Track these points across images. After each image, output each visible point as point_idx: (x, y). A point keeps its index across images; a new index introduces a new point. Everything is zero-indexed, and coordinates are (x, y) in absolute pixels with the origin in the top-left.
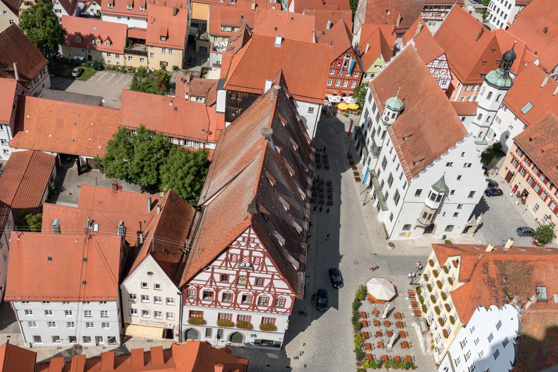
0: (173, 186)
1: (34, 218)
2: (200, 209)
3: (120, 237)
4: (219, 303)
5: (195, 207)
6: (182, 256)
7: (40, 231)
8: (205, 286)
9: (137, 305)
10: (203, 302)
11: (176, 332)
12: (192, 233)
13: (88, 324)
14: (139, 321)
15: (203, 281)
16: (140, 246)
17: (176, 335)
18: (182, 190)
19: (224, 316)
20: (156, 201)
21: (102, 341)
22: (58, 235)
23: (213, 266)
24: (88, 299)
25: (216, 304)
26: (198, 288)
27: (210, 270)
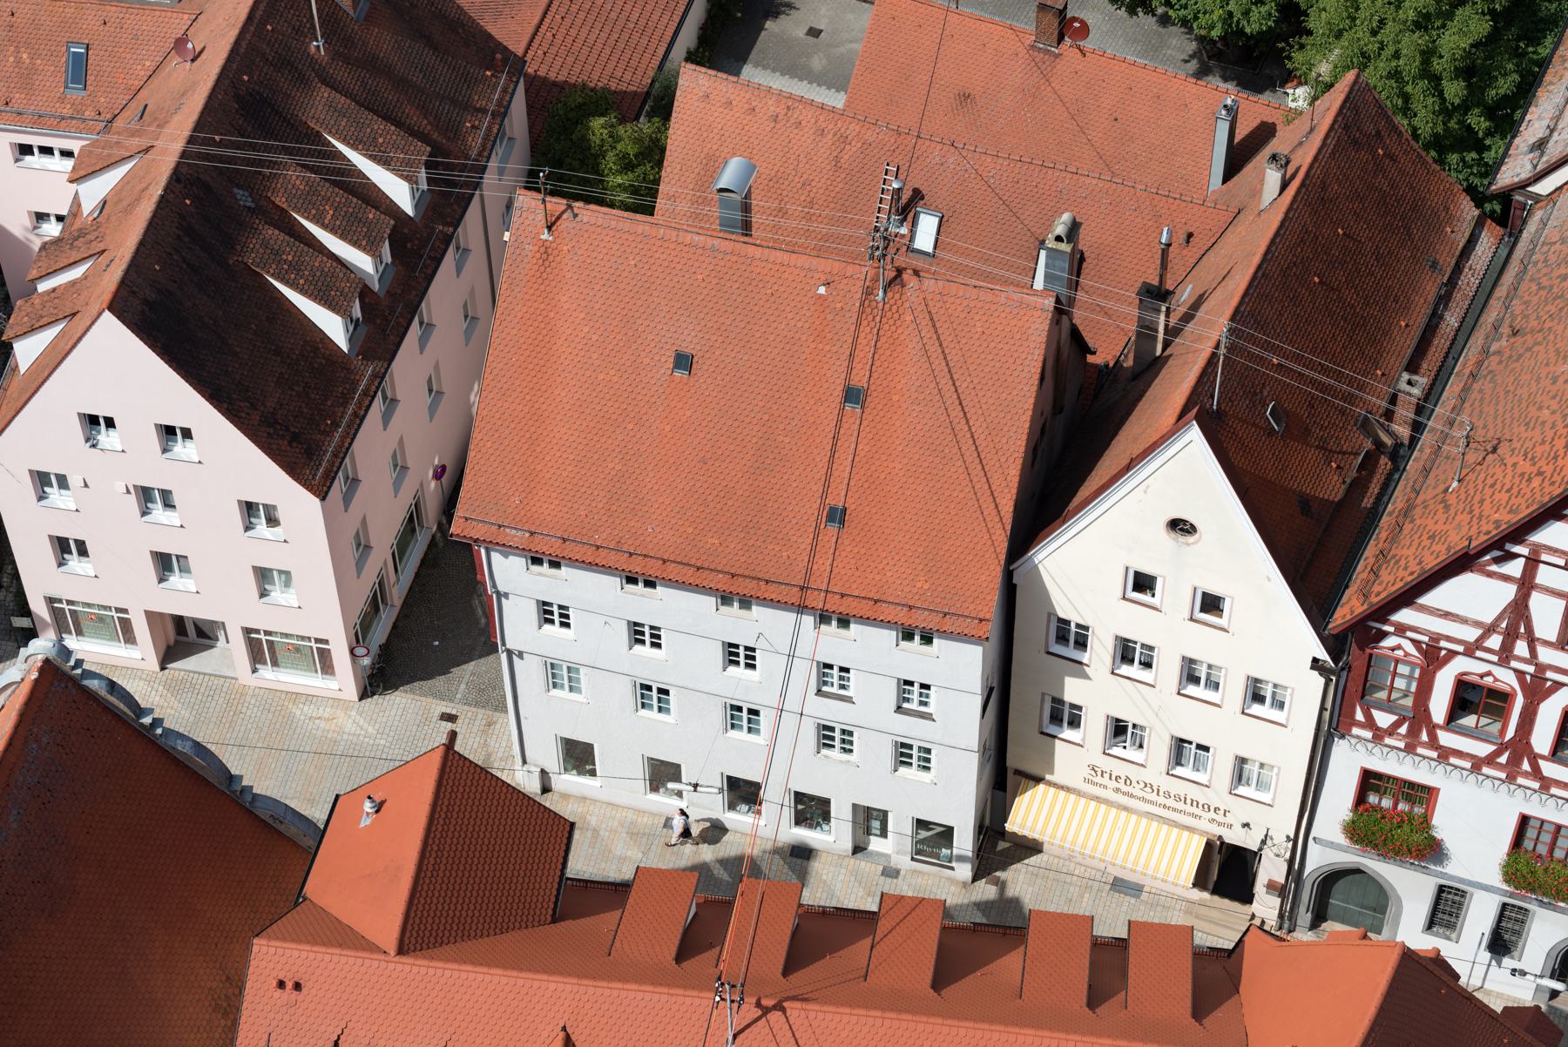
0: (1365, 59)
1: (629, 137)
2: (1506, 211)
3: (1050, 303)
4: (1534, 759)
5: (1479, 199)
6: (1369, 462)
7: (650, 210)
8: (1470, 650)
9: (1095, 690)
10: (1446, 739)
11: (1271, 869)
12: (1440, 344)
13: (826, 735)
14: (1087, 772)
15: (1464, 621)
16: (1148, 367)
17: (1271, 886)
18: (1417, 89)
19: (1546, 838)
20: (1265, 133)
21: (884, 833)
22: (732, 245)
23: (1537, 549)
24: (846, 607)
25: (1514, 762)
26: (1433, 655)
27: (1515, 568)
